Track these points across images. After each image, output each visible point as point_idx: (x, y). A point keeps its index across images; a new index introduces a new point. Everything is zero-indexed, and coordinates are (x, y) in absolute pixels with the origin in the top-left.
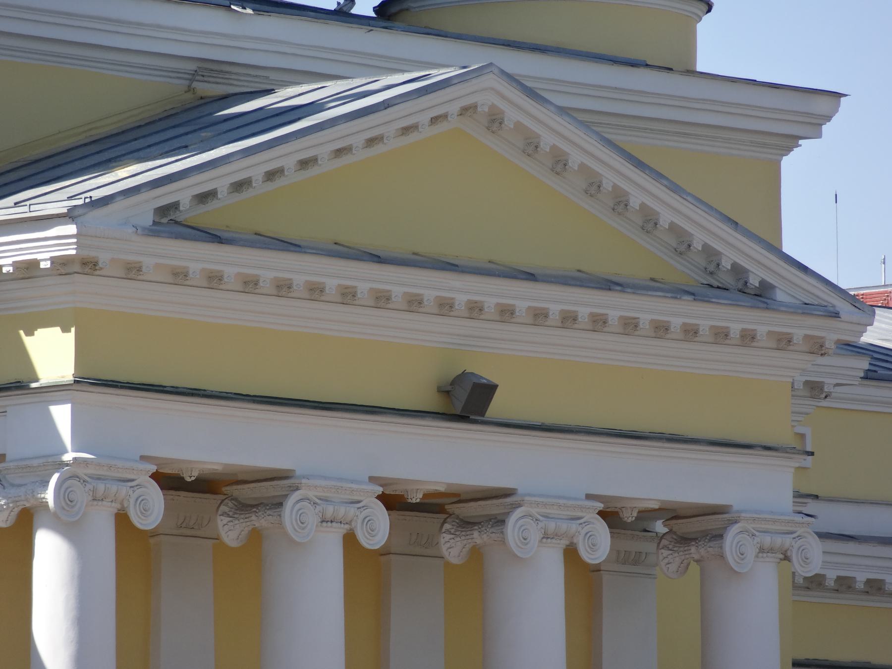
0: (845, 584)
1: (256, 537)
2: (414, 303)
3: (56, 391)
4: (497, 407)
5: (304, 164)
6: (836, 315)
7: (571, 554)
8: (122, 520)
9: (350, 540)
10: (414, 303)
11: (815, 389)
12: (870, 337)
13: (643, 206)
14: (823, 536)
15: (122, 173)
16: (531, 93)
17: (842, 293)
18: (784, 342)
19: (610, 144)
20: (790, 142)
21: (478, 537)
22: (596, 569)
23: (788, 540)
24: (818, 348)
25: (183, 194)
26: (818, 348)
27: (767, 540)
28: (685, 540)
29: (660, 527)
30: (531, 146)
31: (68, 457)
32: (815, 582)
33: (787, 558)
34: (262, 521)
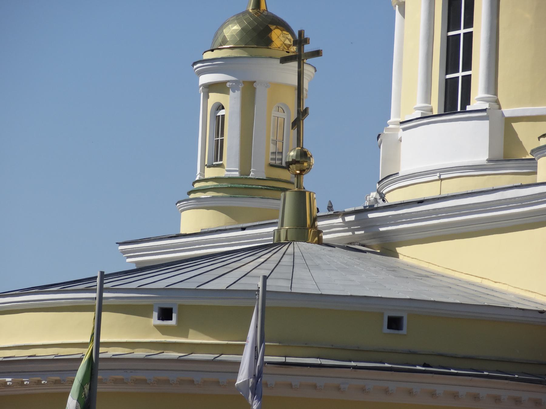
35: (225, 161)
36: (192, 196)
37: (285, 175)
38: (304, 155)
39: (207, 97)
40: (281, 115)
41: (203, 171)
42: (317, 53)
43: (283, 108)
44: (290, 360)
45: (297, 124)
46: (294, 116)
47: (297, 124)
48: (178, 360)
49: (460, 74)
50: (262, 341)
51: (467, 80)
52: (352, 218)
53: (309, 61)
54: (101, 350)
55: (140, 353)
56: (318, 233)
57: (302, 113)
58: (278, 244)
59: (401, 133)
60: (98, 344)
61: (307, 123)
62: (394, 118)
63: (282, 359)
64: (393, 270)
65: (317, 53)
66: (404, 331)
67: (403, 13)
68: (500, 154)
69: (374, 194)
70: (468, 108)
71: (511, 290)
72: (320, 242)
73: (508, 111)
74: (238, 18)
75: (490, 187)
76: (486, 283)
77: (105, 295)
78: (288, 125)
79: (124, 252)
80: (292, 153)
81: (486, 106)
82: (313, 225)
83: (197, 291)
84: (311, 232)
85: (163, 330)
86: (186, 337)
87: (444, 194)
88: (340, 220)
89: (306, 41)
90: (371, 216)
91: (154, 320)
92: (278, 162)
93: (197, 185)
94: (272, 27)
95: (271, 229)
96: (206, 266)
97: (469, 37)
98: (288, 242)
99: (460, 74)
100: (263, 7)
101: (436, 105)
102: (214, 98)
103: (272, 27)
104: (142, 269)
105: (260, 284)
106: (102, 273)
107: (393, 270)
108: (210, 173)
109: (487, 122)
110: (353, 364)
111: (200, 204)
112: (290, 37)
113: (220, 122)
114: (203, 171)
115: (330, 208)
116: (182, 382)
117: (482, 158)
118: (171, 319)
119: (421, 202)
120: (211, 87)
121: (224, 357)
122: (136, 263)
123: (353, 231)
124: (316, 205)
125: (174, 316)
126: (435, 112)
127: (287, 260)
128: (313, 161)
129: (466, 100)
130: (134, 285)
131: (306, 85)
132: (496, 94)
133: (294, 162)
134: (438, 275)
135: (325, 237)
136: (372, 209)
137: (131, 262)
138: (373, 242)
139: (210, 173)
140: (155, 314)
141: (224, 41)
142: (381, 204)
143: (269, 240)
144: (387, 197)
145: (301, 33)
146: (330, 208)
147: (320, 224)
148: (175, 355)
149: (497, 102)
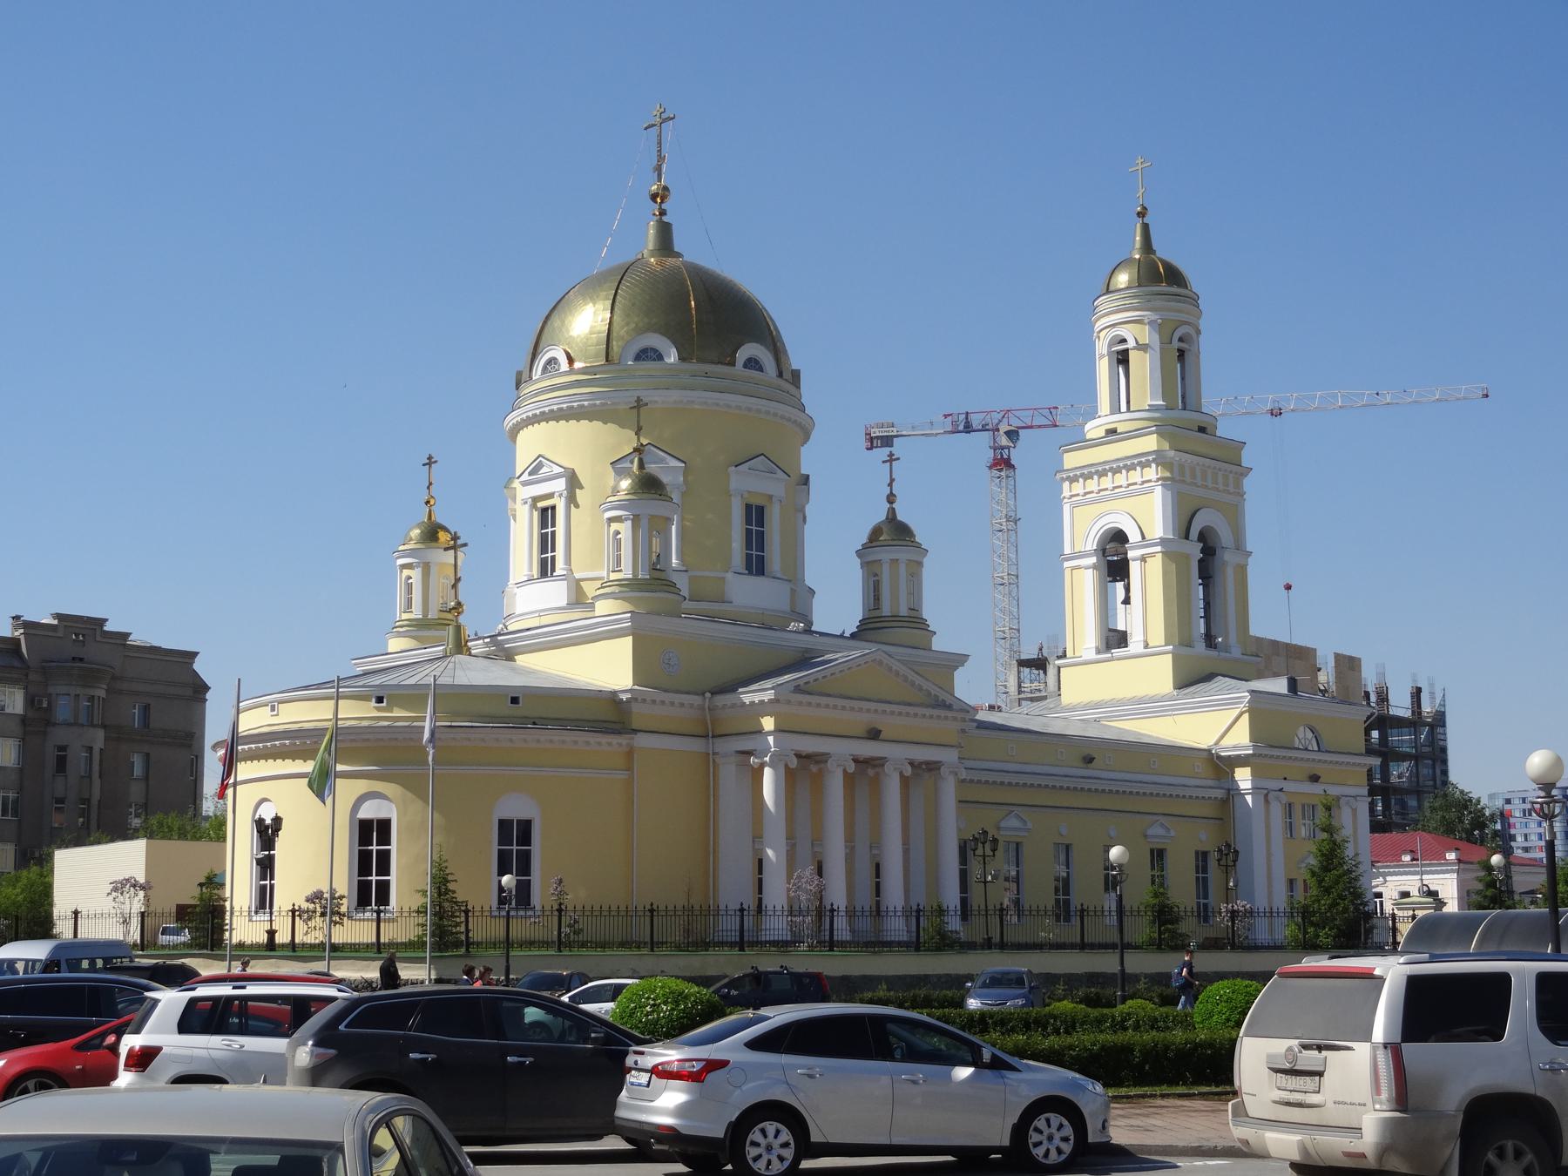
0: (972, 781)
1: (820, 770)
2: (861, 710)
3: (770, 733)
4: (881, 737)
5: (832, 674)
6: (968, 712)
7: (901, 773)
8: (786, 766)
9: (845, 771)
10: (861, 710)
11: (963, 731)
12: (977, 717)
13: (919, 684)
14: (966, 768)
15: (786, 677)
16: (890, 656)
17: (970, 706)
18: (955, 719)
19: (910, 669)
20: (956, 668)
21: (877, 769)
22: (908, 777)
23: (956, 770)
24: (964, 720)
25: (801, 682)
26: (964, 720)
27: (951, 769)
28: (930, 770)
29: (924, 767)
30: (890, 669)
31: (773, 750)
32: (963, 781)
33: (957, 774)
34: (822, 766)
35: (413, 609)
36: (395, 630)
37: (449, 616)
38: (459, 604)
39: (401, 572)
40: (445, 581)
41: (400, 615)
42: (465, 545)
43: (447, 577)
44: (453, 724)
45: (454, 586)
46: (453, 582)
47: (454, 586)
48: (388, 727)
49: (549, 555)
50: (434, 713)
51: (553, 558)
52: (488, 640)
53: (461, 549)
54: (339, 722)
55: (365, 723)
56: (469, 649)
57: (458, 580)
58: (445, 656)
59: (516, 590)
60: (337, 719)
61: (460, 585)
62: (512, 581)
63: (449, 724)
64: (513, 669)
65: (465, 545)
66: (520, 705)
67: (515, 521)
68: (573, 600)
69: (501, 626)
70: (555, 574)
71: (582, 679)
72: (470, 655)
73: (577, 575)
74: (419, 526)
75: (568, 620)
76: (568, 675)
77: (340, 690)
78: (450, 587)
79: (355, 664)
80: (453, 603)
81: (565, 573)
82: (466, 645)
83: (398, 686)
84: (465, 649)
85: (378, 709)
86: (392, 712)
87: (542, 624)
88: (482, 641)
89: (459, 538)
90: (499, 638)
91: (373, 703)
92: (445, 609)
93: (397, 624)
94: (439, 530)
95: (442, 648)
96: (403, 671)
97: (553, 533)
98: (452, 655)
99: (549, 555)
100: (433, 518)
101: (535, 572)
102: (406, 572)
103: (439, 530)
104: (366, 674)
105: (432, 680)
106: (338, 677)
107: (513, 669)
108: (405, 616)
109: (566, 582)
110: (491, 725)
111: (400, 635)
112: (449, 535)
113: (409, 587)
114: (400, 615)
115: (476, 634)
116: (390, 739)
117: (564, 603)
118: (383, 702)
119: (528, 630)
120: (404, 566)
121: (415, 724)
122: (363, 670)
123: (489, 647)
124: (467, 633)
125: (385, 700)
126: (536, 577)
127: (451, 665)
128: (464, 607)
129: (553, 570)
130: (361, 684)
131: (459, 563)
132: (570, 565)
133: (454, 608)
134: (538, 671)
135: (473, 652)
136: (500, 634)
137: (359, 670)
138: (500, 654)
139: (405, 616)
140: (374, 700)
141: (411, 540)
142: (505, 631)
143: (441, 655)
144: (508, 628)
145: (455, 533)
146: (476, 634)
147: (469, 644)
148: (386, 723)
149: (571, 570)
